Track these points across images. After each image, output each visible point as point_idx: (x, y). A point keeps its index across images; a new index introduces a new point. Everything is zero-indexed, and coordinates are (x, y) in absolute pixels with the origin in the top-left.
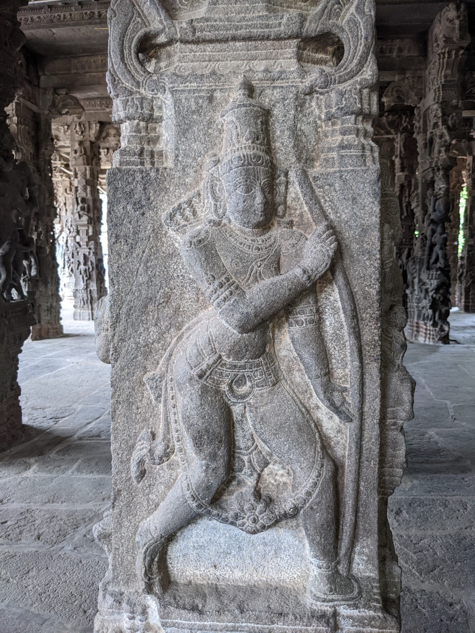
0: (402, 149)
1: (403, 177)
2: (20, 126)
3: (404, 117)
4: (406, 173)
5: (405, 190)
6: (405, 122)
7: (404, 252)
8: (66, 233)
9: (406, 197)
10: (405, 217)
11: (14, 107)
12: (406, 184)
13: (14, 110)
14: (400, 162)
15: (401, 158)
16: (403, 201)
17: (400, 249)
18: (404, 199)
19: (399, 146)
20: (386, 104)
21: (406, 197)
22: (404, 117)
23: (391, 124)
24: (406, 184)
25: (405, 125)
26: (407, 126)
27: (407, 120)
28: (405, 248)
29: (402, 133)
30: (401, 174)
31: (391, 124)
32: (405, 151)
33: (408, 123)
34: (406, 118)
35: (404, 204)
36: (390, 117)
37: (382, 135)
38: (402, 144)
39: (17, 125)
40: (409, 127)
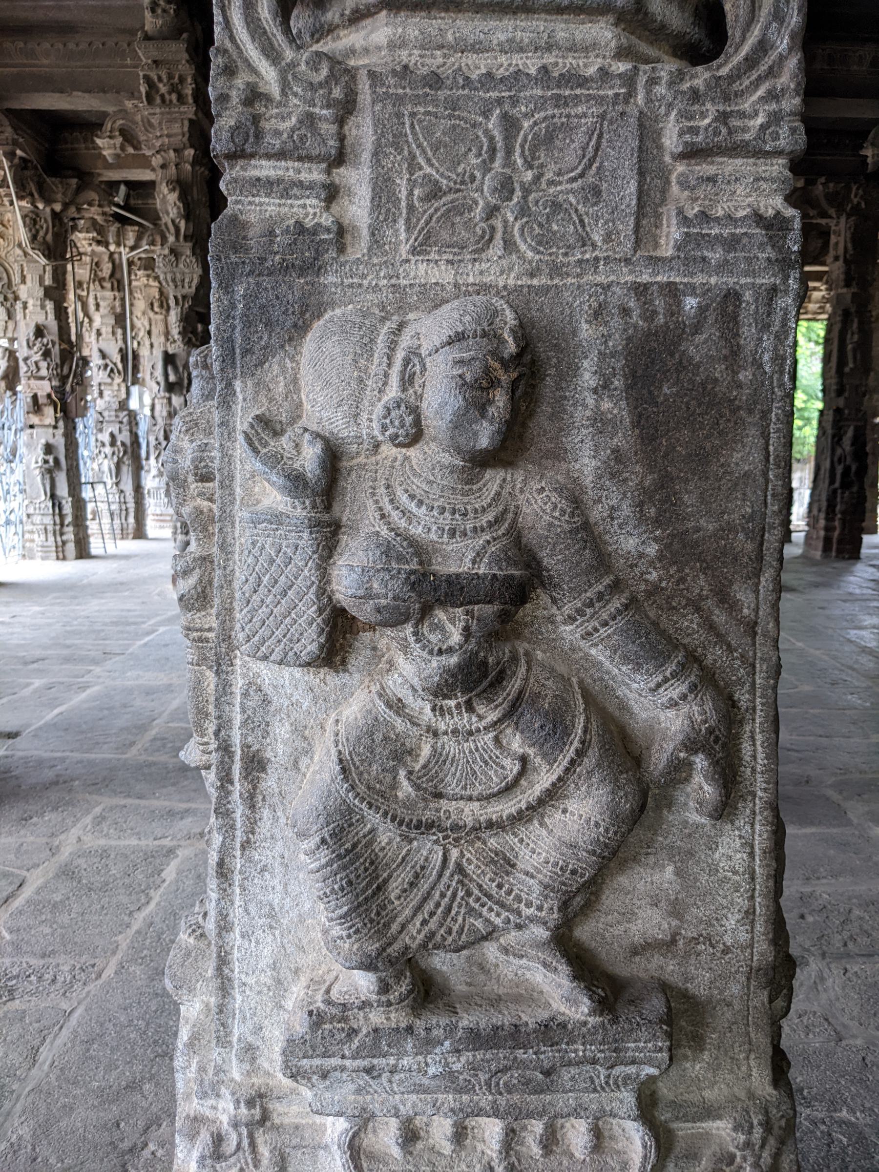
0: (849, 245)
1: (849, 297)
2: (198, 168)
3: (854, 188)
4: (854, 289)
5: (852, 321)
6: (856, 196)
7: (846, 432)
8: (151, 390)
9: (853, 334)
10: (851, 369)
11: (186, 129)
12: (853, 310)
13: (187, 135)
14: (842, 270)
15: (846, 261)
16: (848, 341)
17: (840, 428)
18: (849, 336)
19: (842, 240)
20: (869, 160)
21: (853, 334)
22: (854, 188)
23: (832, 198)
24: (853, 310)
25: (855, 201)
26: (859, 203)
27: (861, 192)
28: (849, 426)
29: (849, 216)
30: (845, 290)
31: (832, 198)
32: (854, 249)
33: (861, 197)
34: (858, 189)
35: (850, 347)
36: (831, 185)
37: (812, 218)
38: (849, 236)
39: (193, 165)
40: (863, 206)
